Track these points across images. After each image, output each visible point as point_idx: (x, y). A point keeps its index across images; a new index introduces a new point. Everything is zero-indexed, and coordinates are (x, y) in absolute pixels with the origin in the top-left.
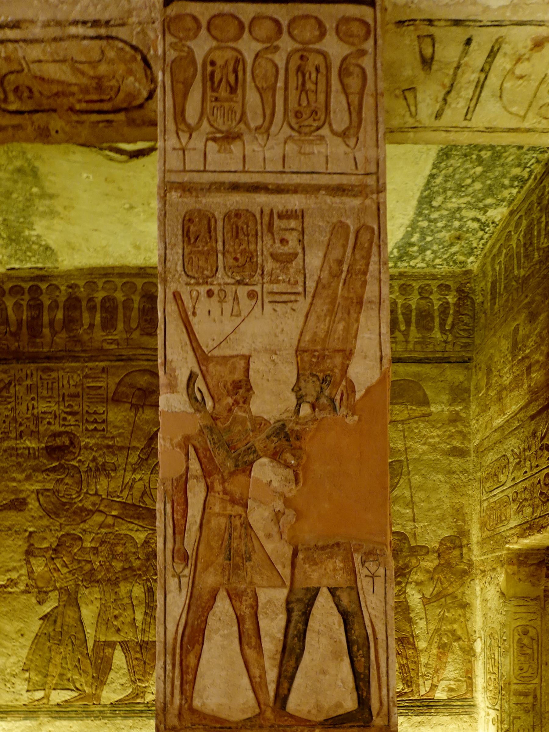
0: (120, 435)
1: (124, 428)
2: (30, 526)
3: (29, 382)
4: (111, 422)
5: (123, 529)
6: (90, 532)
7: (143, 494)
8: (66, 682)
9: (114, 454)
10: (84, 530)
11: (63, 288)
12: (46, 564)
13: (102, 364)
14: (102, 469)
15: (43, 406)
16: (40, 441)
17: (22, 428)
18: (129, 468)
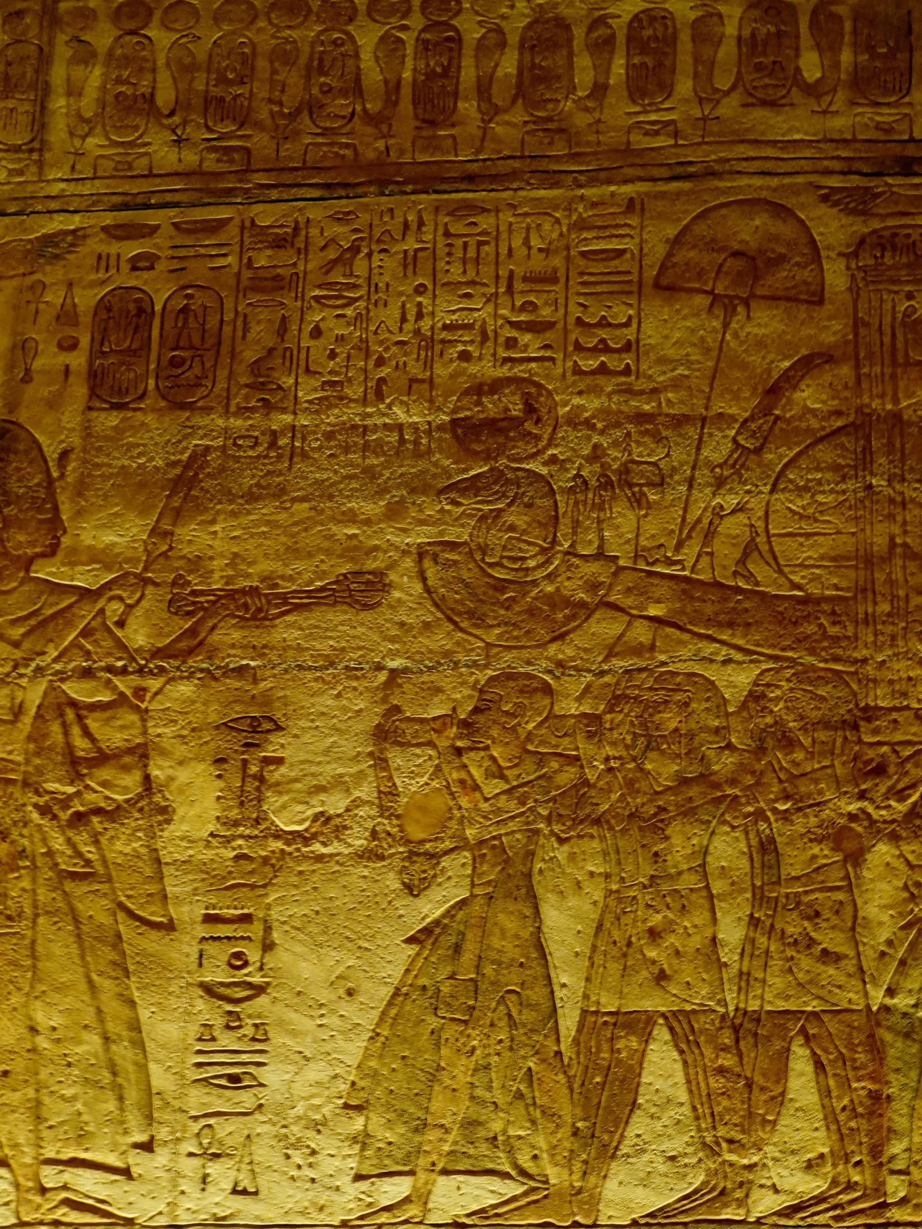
0: (676, 384)
1: (688, 363)
2: (393, 654)
3: (411, 244)
4: (653, 347)
5: (682, 656)
6: (576, 671)
9: (659, 439)
10: (560, 664)
12: (438, 768)
14: (621, 483)
15: (446, 309)
17: (384, 372)
18: (703, 476)
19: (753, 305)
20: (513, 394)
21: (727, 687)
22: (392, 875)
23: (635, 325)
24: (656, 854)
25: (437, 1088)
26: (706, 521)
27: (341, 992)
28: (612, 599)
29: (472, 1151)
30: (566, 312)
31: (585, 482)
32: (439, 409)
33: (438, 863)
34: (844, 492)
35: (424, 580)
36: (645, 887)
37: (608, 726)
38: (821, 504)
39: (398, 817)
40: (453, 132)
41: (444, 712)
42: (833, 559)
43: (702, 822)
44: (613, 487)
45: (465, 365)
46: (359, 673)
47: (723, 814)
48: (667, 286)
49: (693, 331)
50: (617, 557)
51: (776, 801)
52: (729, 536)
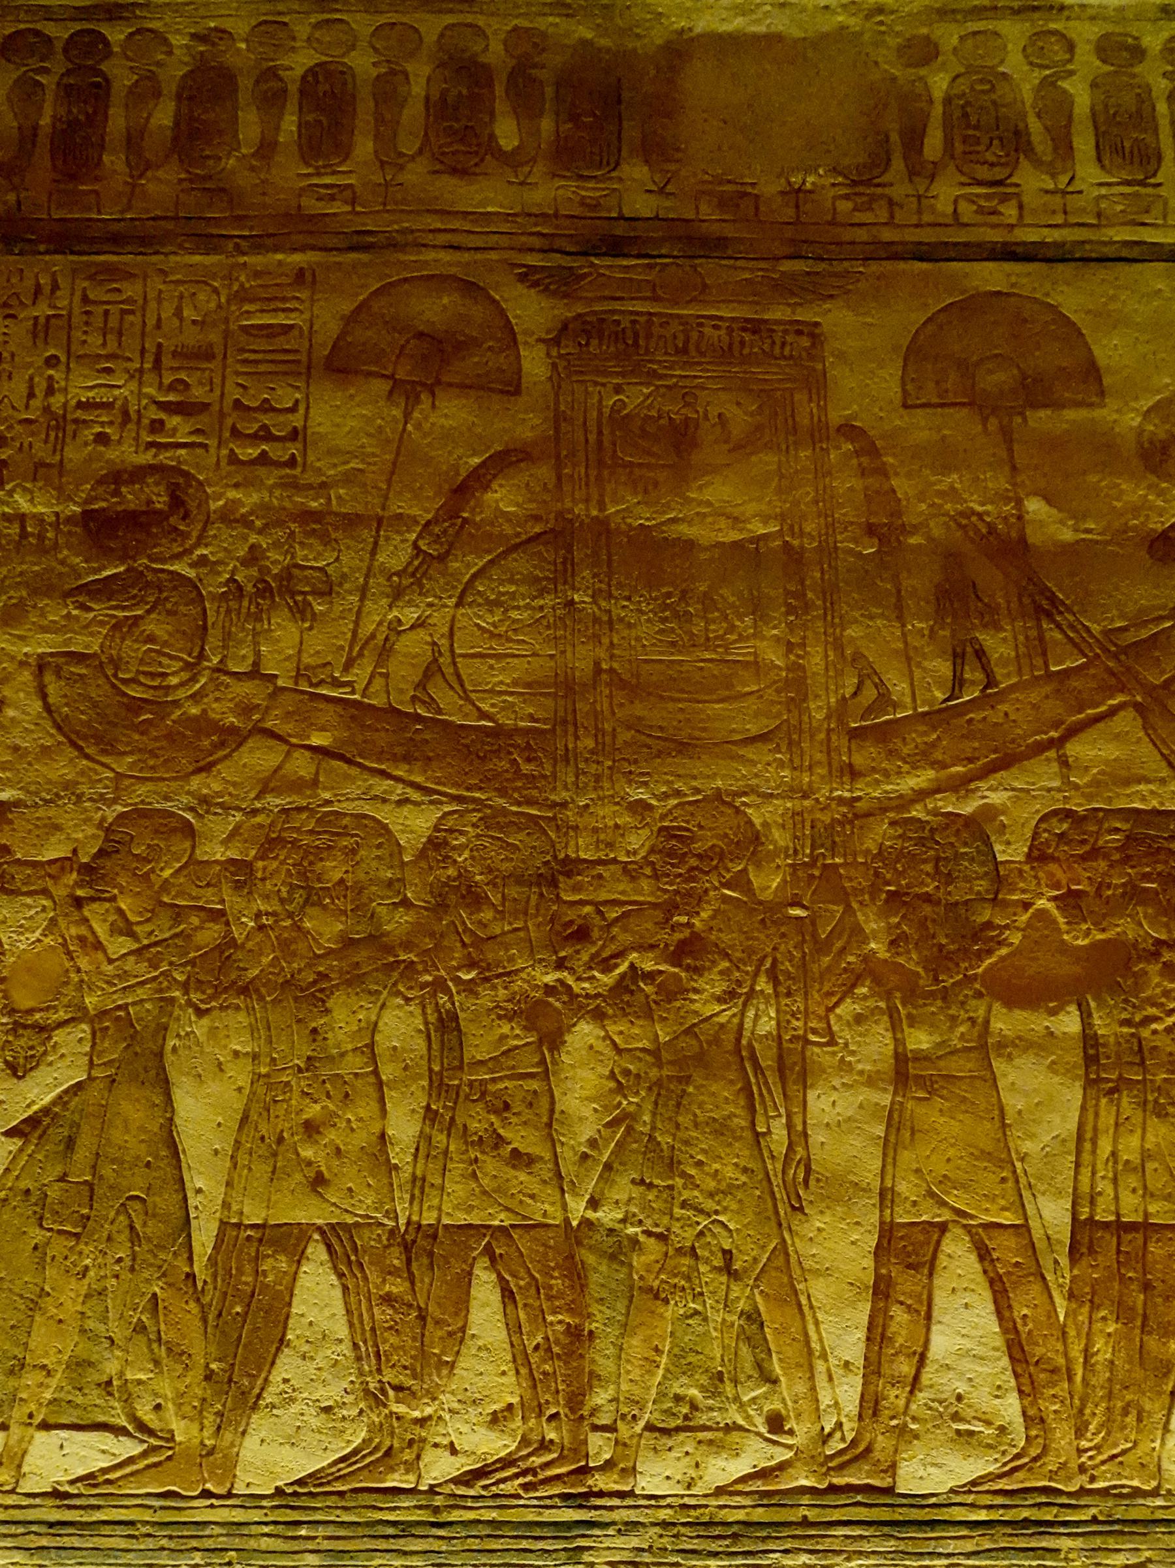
0: (348, 479)
3: (43, 310)
5: (350, 794)
7: (427, 675)
8: (95, 1396)
10: (204, 800)
11: (177, 41)
12: (53, 922)
13: (297, 258)
14: (284, 591)
15: (82, 385)
16: (64, 496)
18: (378, 583)
20: (157, 484)
21: (403, 832)
23: (302, 411)
24: (314, 1031)
25: (37, 1318)
26: (381, 637)
28: (269, 724)
29: (79, 1400)
30: (222, 394)
31: (240, 588)
33: (49, 1038)
34: (541, 608)
35: (44, 697)
36: (300, 1070)
37: (259, 875)
38: (515, 621)
42: (529, 685)
43: (370, 993)
44: (272, 597)
45: (103, 449)
47: (395, 984)
48: (341, 365)
49: (369, 420)
50: (276, 676)
51: (458, 969)
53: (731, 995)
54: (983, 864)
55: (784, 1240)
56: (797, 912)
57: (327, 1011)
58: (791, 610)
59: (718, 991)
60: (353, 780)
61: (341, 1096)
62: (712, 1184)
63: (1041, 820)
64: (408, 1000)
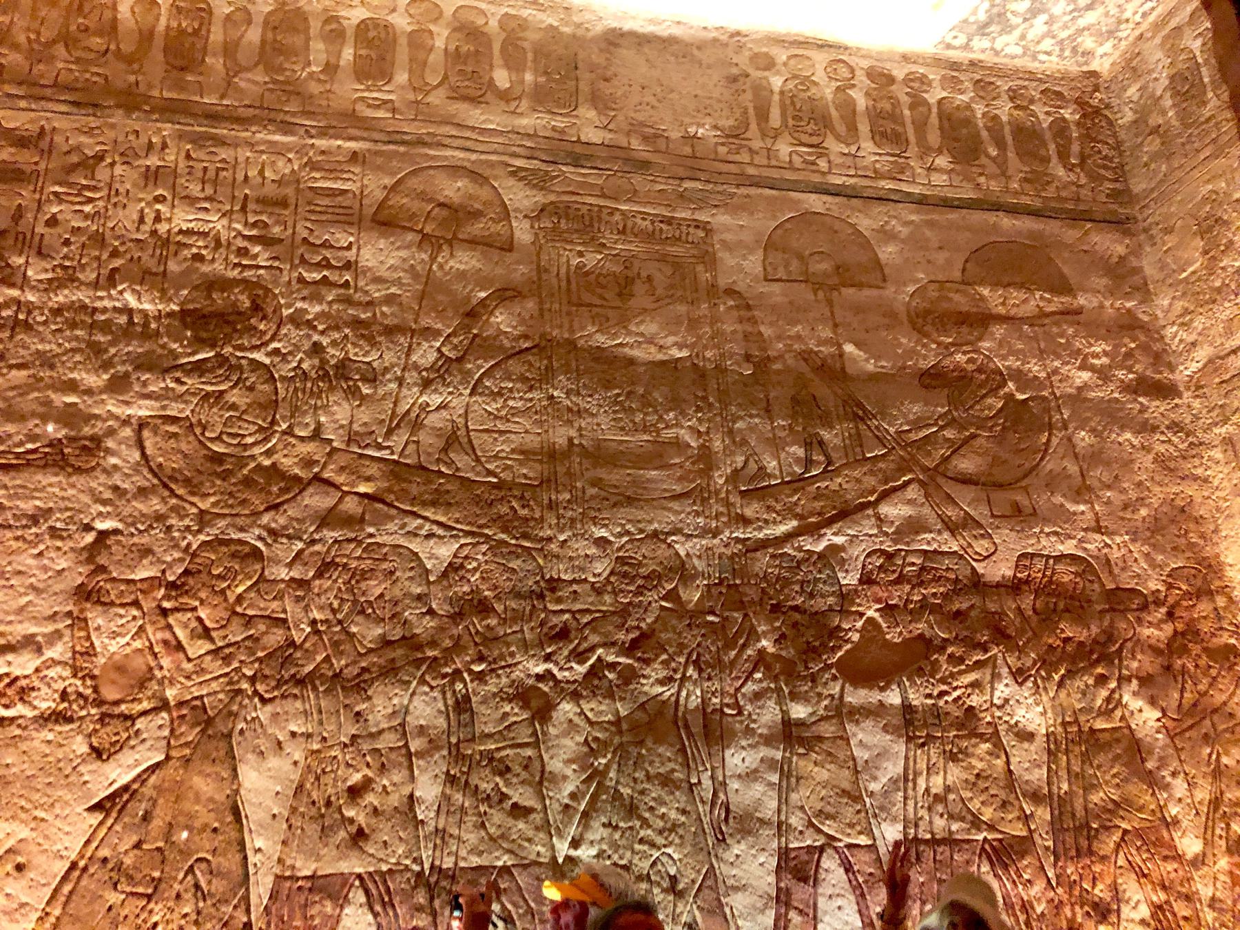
0: (390, 299)
4: (370, 269)
9: (374, 344)
10: (272, 532)
12: (141, 629)
13: (353, 145)
14: (340, 376)
15: (183, 218)
16: (164, 297)
17: (117, 263)
18: (412, 377)
19: (456, 246)
20: (242, 292)
22: (79, 738)
23: (354, 250)
24: (358, 714)
26: (413, 415)
27: (9, 867)
28: (326, 475)
32: (170, 300)
34: (531, 400)
39: (93, 677)
40: (200, 78)
41: (152, 574)
42: (522, 452)
46: (65, 534)
48: (385, 221)
51: (473, 662)
52: (433, 428)
53: (670, 679)
54: (832, 585)
55: (712, 866)
56: (710, 618)
57: (369, 698)
58: (699, 409)
59: (660, 676)
60: (392, 518)
61: (378, 765)
62: (661, 824)
63: (868, 555)
64: (432, 688)
